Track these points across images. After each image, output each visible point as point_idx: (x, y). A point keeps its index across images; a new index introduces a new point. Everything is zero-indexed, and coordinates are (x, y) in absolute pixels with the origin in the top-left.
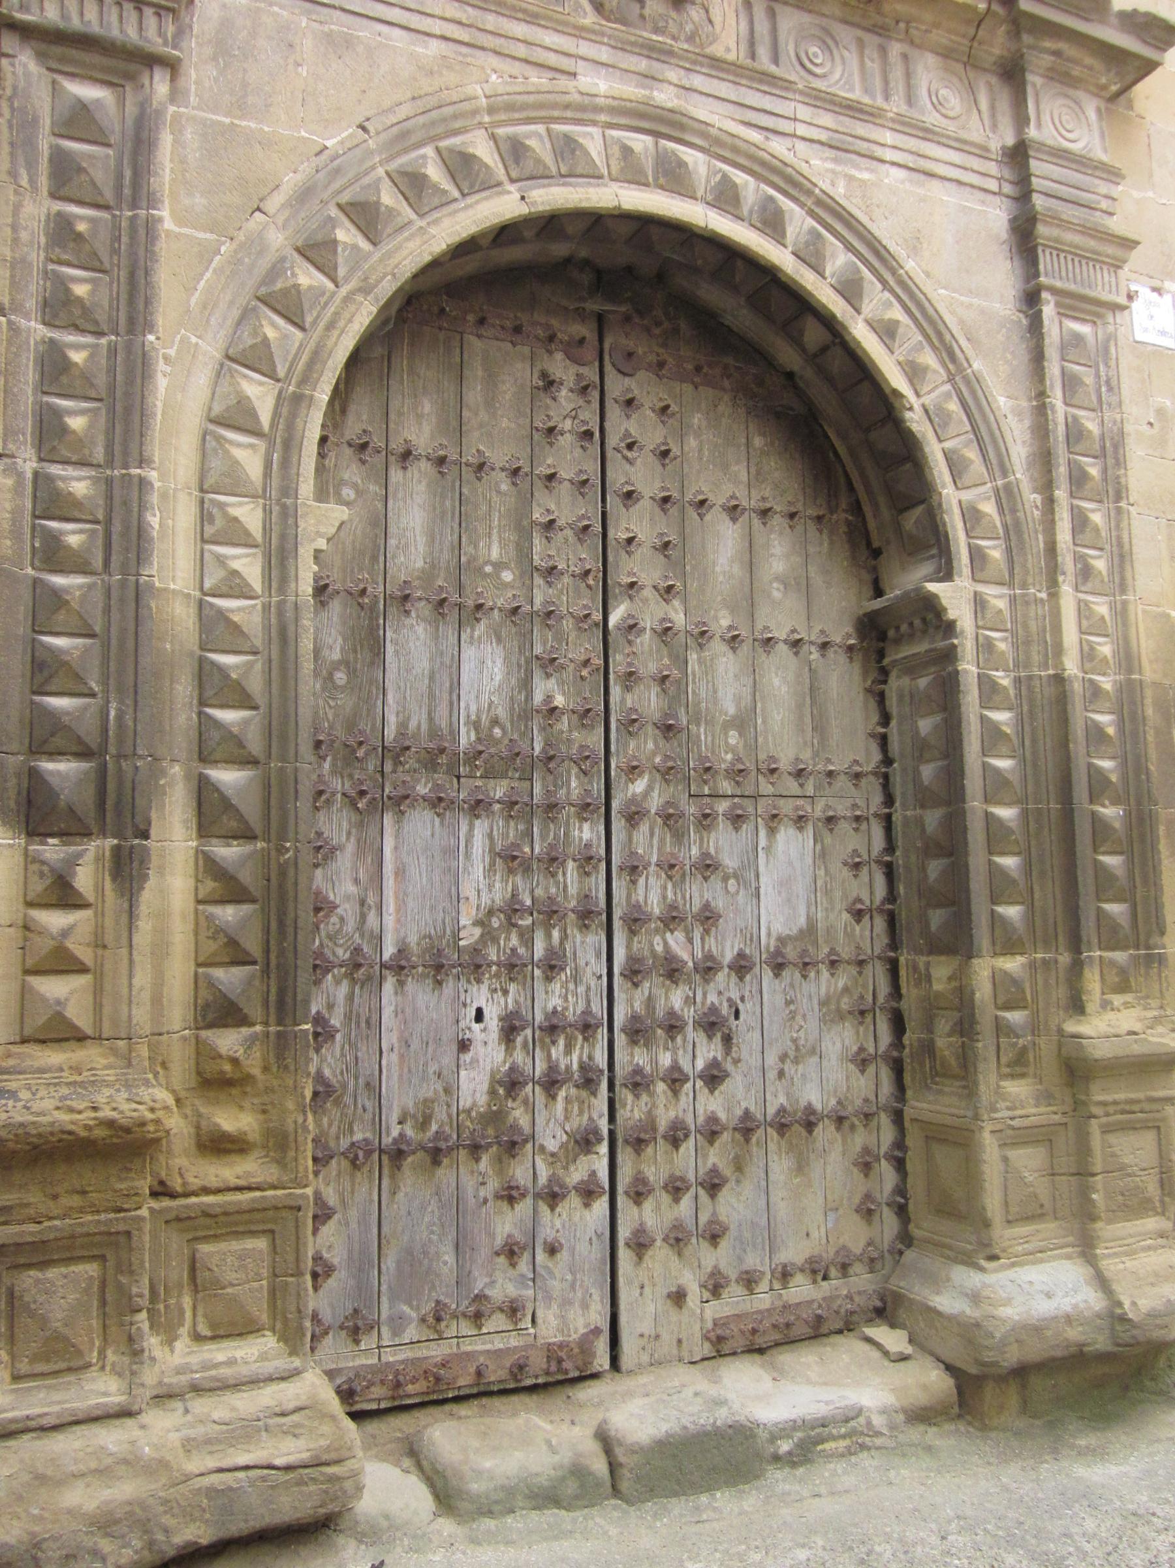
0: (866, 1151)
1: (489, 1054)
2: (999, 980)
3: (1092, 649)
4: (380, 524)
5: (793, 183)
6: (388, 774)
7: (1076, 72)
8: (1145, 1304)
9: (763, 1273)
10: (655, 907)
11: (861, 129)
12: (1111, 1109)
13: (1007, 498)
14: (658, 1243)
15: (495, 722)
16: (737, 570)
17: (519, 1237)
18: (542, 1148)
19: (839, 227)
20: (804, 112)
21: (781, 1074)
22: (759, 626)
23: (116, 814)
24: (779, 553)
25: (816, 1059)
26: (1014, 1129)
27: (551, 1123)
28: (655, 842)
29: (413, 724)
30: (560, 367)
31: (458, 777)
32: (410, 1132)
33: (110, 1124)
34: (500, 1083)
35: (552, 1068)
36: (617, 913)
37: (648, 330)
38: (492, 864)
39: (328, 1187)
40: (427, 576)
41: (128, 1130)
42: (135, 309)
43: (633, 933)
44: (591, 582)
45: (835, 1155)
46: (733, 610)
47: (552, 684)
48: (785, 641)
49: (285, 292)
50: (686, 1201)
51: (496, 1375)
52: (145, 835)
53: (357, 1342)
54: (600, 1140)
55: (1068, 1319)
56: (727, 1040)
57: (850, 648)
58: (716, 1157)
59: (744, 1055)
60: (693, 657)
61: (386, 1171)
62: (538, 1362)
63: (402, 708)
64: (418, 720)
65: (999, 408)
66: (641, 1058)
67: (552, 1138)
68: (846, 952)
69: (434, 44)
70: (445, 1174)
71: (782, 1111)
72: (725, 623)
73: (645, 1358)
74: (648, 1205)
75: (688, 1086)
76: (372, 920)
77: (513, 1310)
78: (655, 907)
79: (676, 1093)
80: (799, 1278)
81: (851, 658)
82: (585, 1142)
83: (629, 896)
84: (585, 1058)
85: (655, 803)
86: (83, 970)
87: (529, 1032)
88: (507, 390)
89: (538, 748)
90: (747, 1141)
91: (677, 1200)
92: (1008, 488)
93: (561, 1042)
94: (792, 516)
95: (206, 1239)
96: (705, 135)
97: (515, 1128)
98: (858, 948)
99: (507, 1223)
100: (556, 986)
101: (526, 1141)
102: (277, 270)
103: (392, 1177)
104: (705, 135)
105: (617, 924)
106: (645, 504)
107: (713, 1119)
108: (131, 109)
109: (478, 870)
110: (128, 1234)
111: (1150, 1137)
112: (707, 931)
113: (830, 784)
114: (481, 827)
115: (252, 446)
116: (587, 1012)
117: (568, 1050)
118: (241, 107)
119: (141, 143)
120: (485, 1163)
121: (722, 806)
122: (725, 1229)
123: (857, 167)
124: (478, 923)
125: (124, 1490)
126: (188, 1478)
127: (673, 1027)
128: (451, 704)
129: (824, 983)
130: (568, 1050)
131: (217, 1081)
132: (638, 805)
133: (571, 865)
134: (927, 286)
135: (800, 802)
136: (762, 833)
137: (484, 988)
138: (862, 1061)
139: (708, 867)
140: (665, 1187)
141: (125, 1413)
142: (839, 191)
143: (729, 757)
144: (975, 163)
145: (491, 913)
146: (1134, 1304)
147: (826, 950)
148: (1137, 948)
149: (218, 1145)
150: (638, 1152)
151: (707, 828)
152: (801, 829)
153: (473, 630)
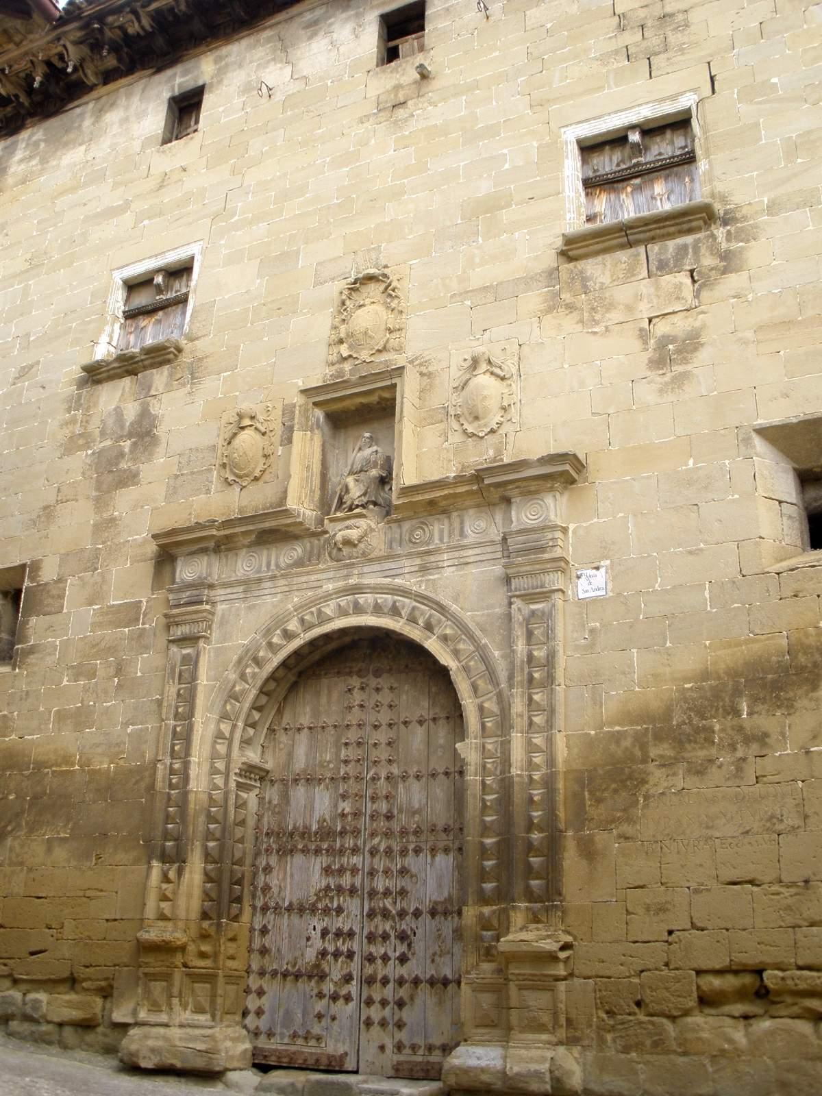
1: (318, 944)
2: (481, 916)
4: (290, 755)
5: (405, 592)
7: (533, 488)
8: (516, 1069)
9: (420, 1047)
11: (432, 559)
12: (521, 978)
13: (500, 695)
15: (325, 820)
16: (422, 747)
17: (323, 1013)
19: (425, 602)
21: (433, 961)
23: (177, 858)
27: (336, 970)
30: (355, 681)
32: (290, 968)
33: (163, 941)
35: (337, 949)
39: (265, 983)
40: (305, 771)
42: (191, 714)
43: (371, 899)
50: (388, 1009)
51: (311, 1061)
52: (184, 862)
55: (483, 1070)
56: (409, 945)
58: (403, 992)
59: (417, 952)
60: (401, 786)
62: (324, 1061)
63: (294, 819)
64: (300, 823)
66: (373, 949)
71: (432, 976)
72: (415, 770)
73: (368, 1070)
74: (373, 1008)
75: (391, 962)
76: (282, 894)
77: (319, 1039)
82: (348, 979)
88: (335, 695)
89: (339, 829)
91: (384, 1008)
93: (341, 940)
95: (197, 982)
96: (369, 588)
97: (323, 971)
99: (320, 1006)
100: (340, 919)
104: (369, 588)
105: (366, 895)
106: (384, 727)
107: (402, 977)
109: (317, 876)
111: (549, 994)
112: (403, 899)
114: (319, 859)
116: (351, 929)
117: (343, 944)
118: (225, 640)
120: (313, 983)
121: (411, 847)
122: (405, 1024)
123: (432, 574)
124: (316, 895)
125: (160, 1043)
126: (175, 1046)
130: (343, 944)
131: (204, 936)
133: (348, 873)
136: (429, 857)
137: (316, 919)
139: (404, 871)
141: (166, 1025)
142: (422, 589)
144: (489, 549)
146: (511, 1068)
149: (203, 955)
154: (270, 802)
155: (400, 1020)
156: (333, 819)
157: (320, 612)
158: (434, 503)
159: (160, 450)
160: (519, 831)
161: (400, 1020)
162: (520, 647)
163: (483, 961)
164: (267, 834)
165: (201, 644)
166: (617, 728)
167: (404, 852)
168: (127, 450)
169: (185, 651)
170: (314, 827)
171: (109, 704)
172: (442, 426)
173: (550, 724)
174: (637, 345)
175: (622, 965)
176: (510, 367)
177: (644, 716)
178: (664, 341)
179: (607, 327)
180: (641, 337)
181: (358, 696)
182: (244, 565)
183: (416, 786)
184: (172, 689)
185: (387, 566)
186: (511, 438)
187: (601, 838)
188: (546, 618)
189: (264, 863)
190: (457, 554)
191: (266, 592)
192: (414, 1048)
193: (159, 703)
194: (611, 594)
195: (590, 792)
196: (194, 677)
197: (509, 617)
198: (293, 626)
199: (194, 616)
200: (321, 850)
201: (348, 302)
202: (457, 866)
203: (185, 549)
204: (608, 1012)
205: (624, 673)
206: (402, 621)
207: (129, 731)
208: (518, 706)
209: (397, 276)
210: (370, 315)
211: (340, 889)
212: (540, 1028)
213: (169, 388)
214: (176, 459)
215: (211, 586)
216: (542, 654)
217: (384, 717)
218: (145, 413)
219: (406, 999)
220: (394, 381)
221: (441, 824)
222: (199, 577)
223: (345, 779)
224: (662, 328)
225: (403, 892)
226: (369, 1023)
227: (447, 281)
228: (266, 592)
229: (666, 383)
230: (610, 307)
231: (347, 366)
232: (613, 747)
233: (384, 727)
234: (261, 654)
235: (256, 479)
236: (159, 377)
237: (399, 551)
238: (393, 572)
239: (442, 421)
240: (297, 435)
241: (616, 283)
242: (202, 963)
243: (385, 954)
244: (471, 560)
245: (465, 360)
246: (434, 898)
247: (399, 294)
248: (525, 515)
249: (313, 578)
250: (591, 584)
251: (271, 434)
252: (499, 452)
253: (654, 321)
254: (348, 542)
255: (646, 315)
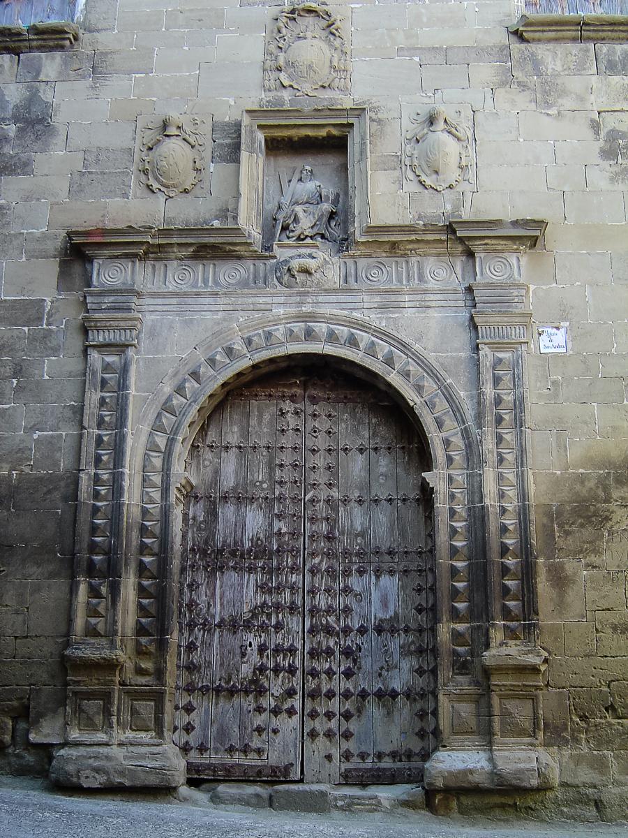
0: (422, 710)
1: (254, 658)
3: (503, 493)
4: (217, 472)
5: (364, 327)
6: (215, 557)
7: (499, 247)
9: (369, 755)
10: (323, 606)
11: (393, 298)
13: (466, 433)
14: (321, 735)
15: (259, 539)
16: (363, 474)
18: (273, 694)
19: (385, 338)
20: (366, 298)
22: (373, 494)
23: (112, 572)
24: (384, 464)
25: (398, 670)
26: (455, 694)
27: (276, 686)
28: (324, 581)
29: (228, 541)
30: (288, 406)
31: (245, 559)
33: (104, 659)
34: (257, 669)
35: (277, 665)
36: (307, 608)
37: (324, 386)
38: (257, 590)
40: (234, 489)
41: (109, 661)
42: (121, 422)
43: (312, 617)
44: (299, 485)
45: (406, 711)
46: (361, 489)
47: (282, 524)
48: (385, 500)
49: (170, 406)
53: (202, 754)
54: (296, 694)
57: (418, 500)
60: (341, 509)
61: (214, 696)
64: (230, 540)
65: (461, 397)
67: (277, 690)
68: (413, 626)
69: (220, 313)
70: (236, 700)
71: (380, 689)
72: (357, 495)
73: (314, 779)
75: (336, 676)
77: (259, 751)
78: (323, 606)
79: (330, 679)
80: (387, 759)
81: (419, 505)
82: (291, 693)
83: (312, 602)
84: (291, 662)
85: (324, 566)
86: (103, 617)
87: (269, 651)
88: (267, 417)
89: (275, 548)
90: (364, 700)
92: (465, 428)
94: (389, 448)
95: (136, 700)
97: (262, 686)
98: (419, 625)
99: (259, 720)
100: (280, 635)
101: (266, 691)
102: (169, 399)
103: (216, 699)
105: (307, 613)
106: (322, 452)
107: (348, 690)
108: (123, 361)
109: (252, 593)
110: (110, 693)
111: (529, 704)
113: (406, 557)
115: (159, 456)
117: (284, 659)
119: (125, 370)
121: (355, 567)
122: (352, 735)
126: (122, 764)
127: (329, 652)
128: (242, 532)
129: (400, 639)
130: (284, 659)
132: (316, 568)
133: (288, 591)
134: (425, 353)
135: (391, 564)
136: (373, 578)
138: (420, 672)
139: (347, 590)
140: (325, 714)
141: (107, 745)
143: (358, 548)
144: (451, 297)
145: (256, 608)
147: (404, 625)
148: (525, 621)
149: (140, 671)
150: (313, 700)
151: (348, 576)
152: (392, 575)
153: (251, 506)
154: (194, 518)
155: (347, 730)
156: (269, 538)
157: (269, 335)
158: (393, 243)
159: (60, 140)
160: (494, 555)
161: (347, 730)
162: (488, 390)
163: (457, 674)
164: (193, 550)
165: (131, 352)
166: (581, 471)
167: (347, 573)
168: (12, 134)
169: (109, 359)
170: (247, 545)
171: (8, 406)
172: (397, 173)
173: (521, 461)
174: (589, 134)
175: (593, 676)
176: (465, 130)
177: (607, 463)
178: (613, 136)
179: (559, 112)
180: (593, 127)
181: (291, 421)
182: (176, 276)
183: (357, 510)
184: (93, 397)
185: (343, 298)
186: (468, 196)
187: (570, 565)
188: (516, 364)
189: (189, 580)
190: (419, 297)
191: (206, 308)
192: (363, 756)
193: (79, 411)
194: (571, 353)
195: (561, 526)
196: (123, 385)
197: (477, 364)
198: (239, 346)
199: (122, 324)
200: (256, 569)
201: (284, 31)
202: (402, 586)
203: (107, 252)
204: (580, 717)
205: (585, 423)
206: (361, 354)
207: (35, 436)
208: (489, 444)
209: (339, 17)
210: (311, 49)
211: (278, 607)
212: (522, 733)
213: (63, 77)
214: (80, 155)
215: (139, 295)
216: (510, 398)
217: (322, 442)
218: (33, 98)
219: (353, 711)
220: (351, 121)
221: (384, 549)
222: (124, 284)
223: (281, 498)
224: (610, 122)
225: (347, 610)
226: (313, 734)
227: (393, 33)
228: (206, 308)
229: (616, 174)
230: (564, 93)
231: (286, 95)
232: (578, 487)
233: (322, 452)
234: (202, 370)
235: (186, 191)
236: (51, 64)
237: (355, 286)
238: (351, 306)
239: (395, 169)
240: (244, 155)
241: (567, 73)
242: (143, 680)
243: (330, 668)
244: (434, 304)
245: (418, 114)
246: (381, 615)
247: (342, 34)
248: (491, 270)
249: (261, 300)
250: (553, 341)
251: (201, 148)
252: (456, 208)
253: (602, 114)
254: (306, 271)
255: (596, 109)
